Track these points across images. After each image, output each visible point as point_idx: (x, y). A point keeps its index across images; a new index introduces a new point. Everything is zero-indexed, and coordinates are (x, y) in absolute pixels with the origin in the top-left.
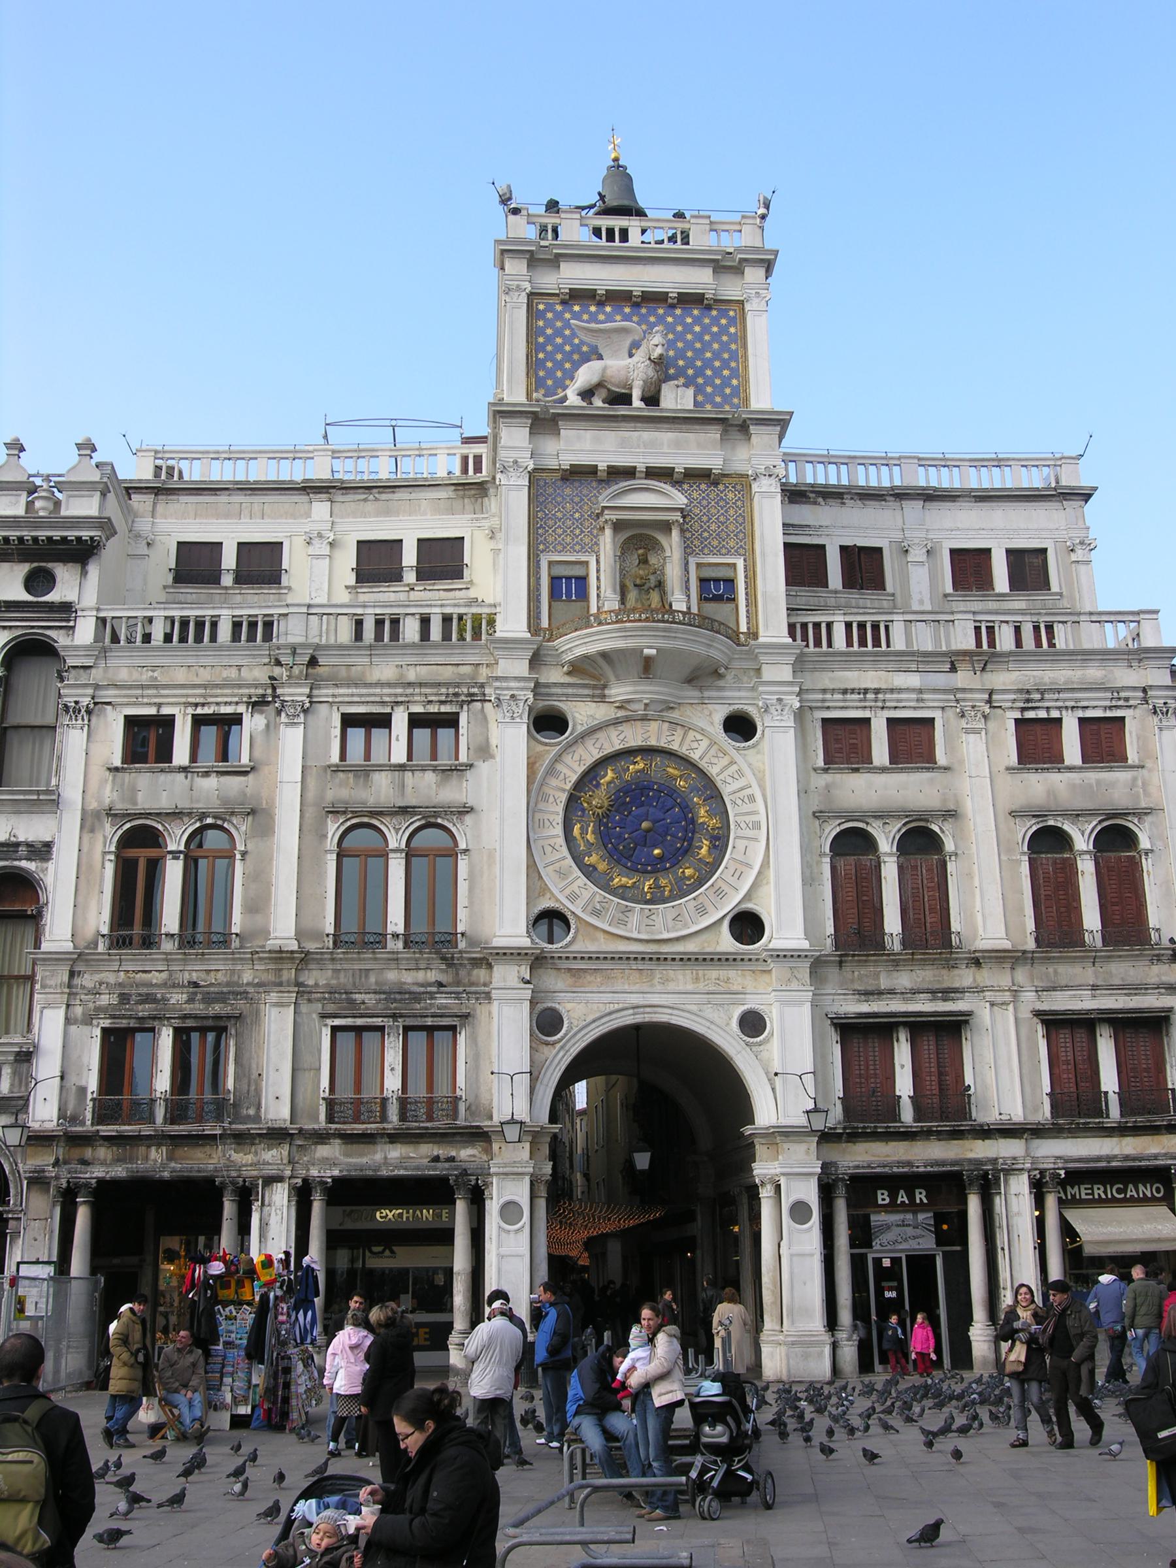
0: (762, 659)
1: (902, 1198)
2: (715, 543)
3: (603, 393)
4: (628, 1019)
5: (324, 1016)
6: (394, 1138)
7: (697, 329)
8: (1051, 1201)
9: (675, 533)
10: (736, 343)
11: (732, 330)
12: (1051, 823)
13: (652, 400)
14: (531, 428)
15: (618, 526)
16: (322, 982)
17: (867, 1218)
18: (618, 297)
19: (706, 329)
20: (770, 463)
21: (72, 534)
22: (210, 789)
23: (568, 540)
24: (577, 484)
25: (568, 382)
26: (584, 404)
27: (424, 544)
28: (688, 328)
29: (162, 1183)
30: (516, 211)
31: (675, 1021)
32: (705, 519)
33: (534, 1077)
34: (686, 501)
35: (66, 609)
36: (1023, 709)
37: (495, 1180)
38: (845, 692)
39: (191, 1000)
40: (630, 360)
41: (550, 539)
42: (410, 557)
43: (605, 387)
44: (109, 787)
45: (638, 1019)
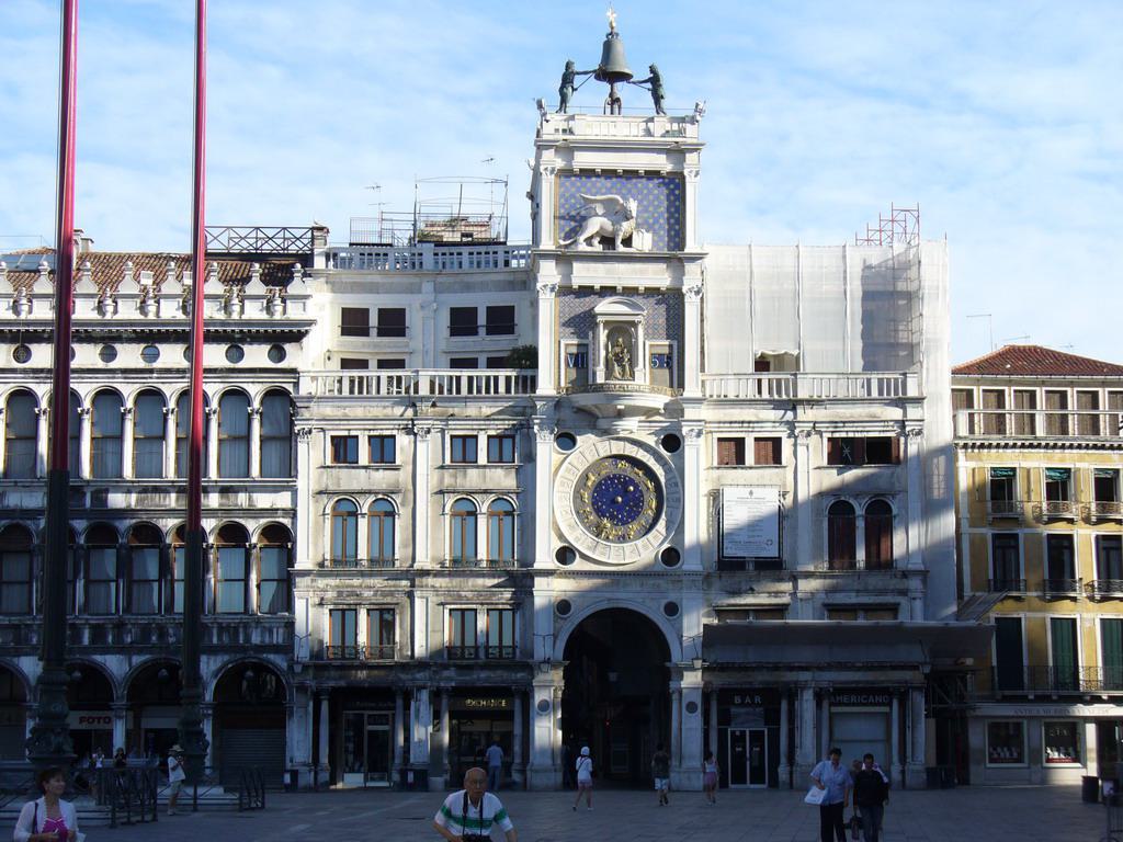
0: (684, 405)
1: (748, 700)
4: (605, 606)
5: (443, 604)
6: (484, 667)
7: (656, 192)
8: (825, 704)
11: (677, 192)
12: (843, 498)
13: (627, 242)
15: (606, 324)
16: (444, 585)
17: (729, 710)
18: (609, 174)
21: (295, 329)
22: (381, 478)
27: (490, 310)
29: (364, 688)
31: (631, 607)
33: (555, 637)
35: (294, 371)
36: (833, 432)
37: (536, 689)
38: (731, 423)
39: (375, 595)
42: (482, 319)
44: (325, 477)
45: (611, 606)
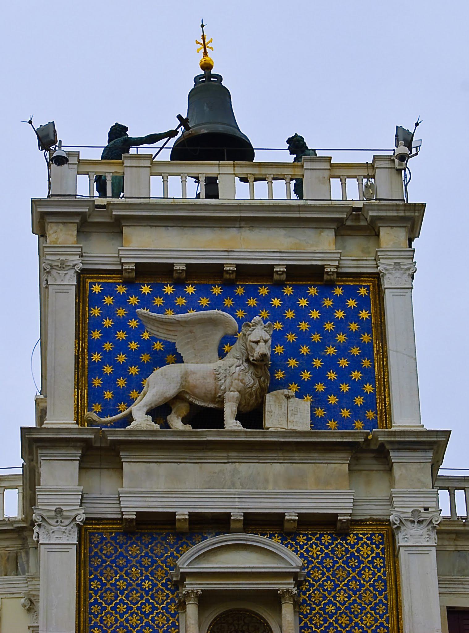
2: (344, 620)
3: (184, 409)
7: (315, 314)
9: (288, 610)
10: (369, 332)
11: (364, 315)
13: (252, 416)
14: (81, 462)
15: (205, 600)
18: (203, 274)
19: (327, 315)
20: (419, 505)
23: (135, 620)
24: (146, 539)
25: (134, 394)
26: (157, 427)
28: (302, 314)
30: (60, 161)
32: (329, 585)
34: (300, 562)
40: (220, 363)
41: (110, 620)
43: (184, 400)
